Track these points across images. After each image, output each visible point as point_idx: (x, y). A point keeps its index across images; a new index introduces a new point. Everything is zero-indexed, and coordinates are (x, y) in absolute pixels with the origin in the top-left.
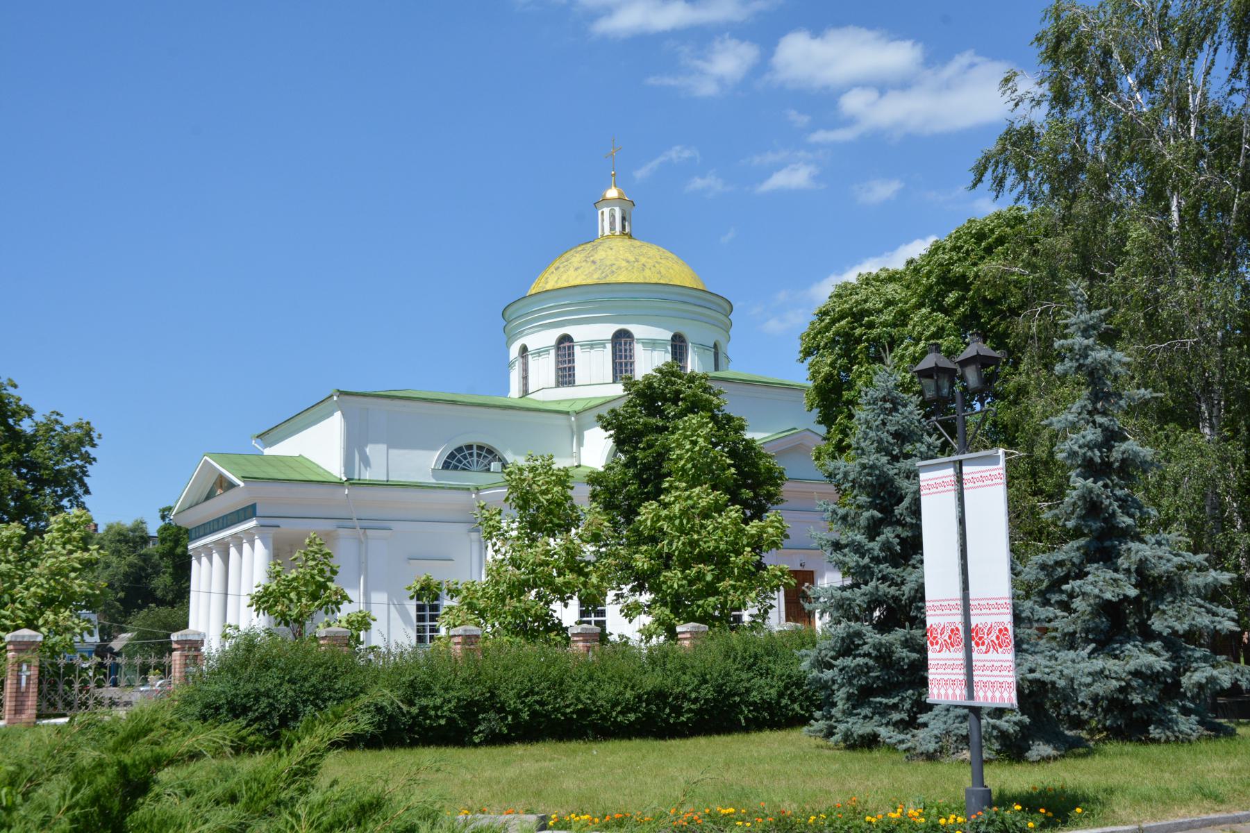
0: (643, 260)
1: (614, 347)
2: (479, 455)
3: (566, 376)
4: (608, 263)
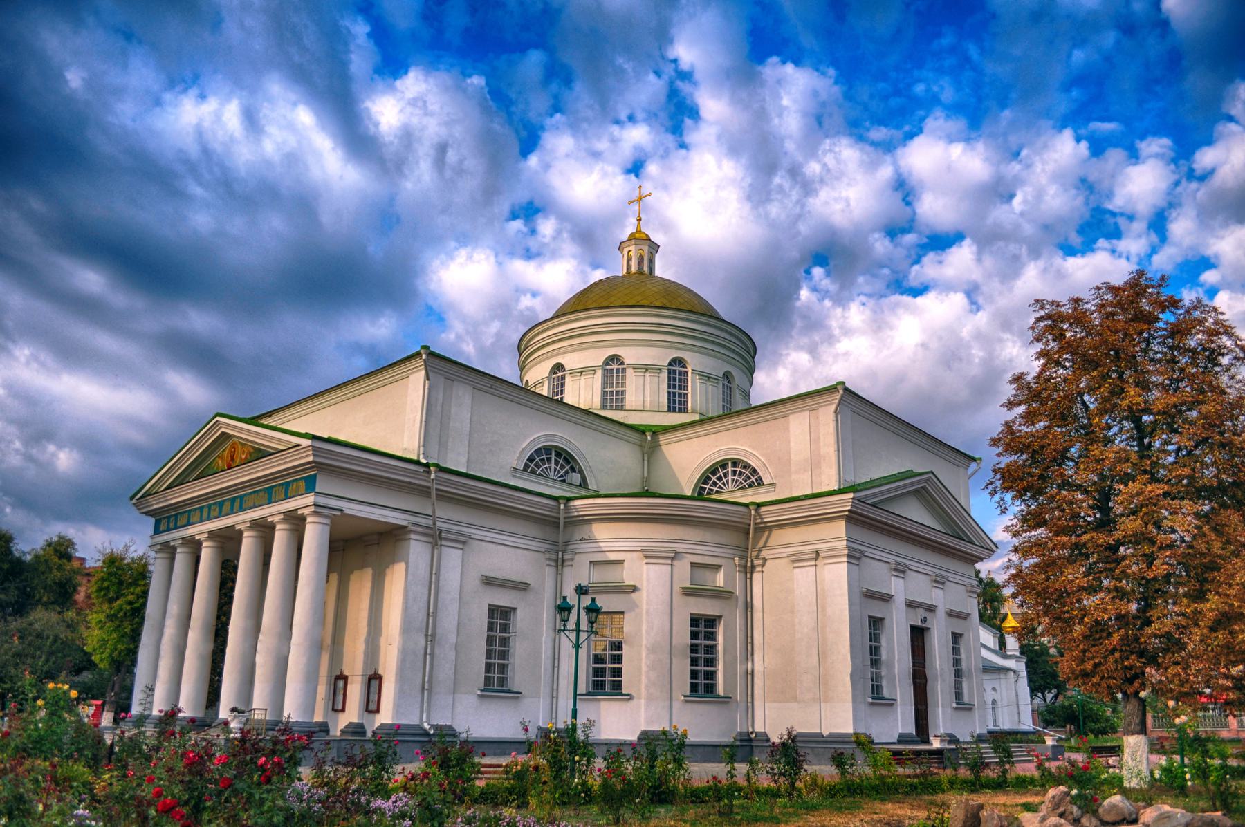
2: (557, 463)
3: (614, 397)
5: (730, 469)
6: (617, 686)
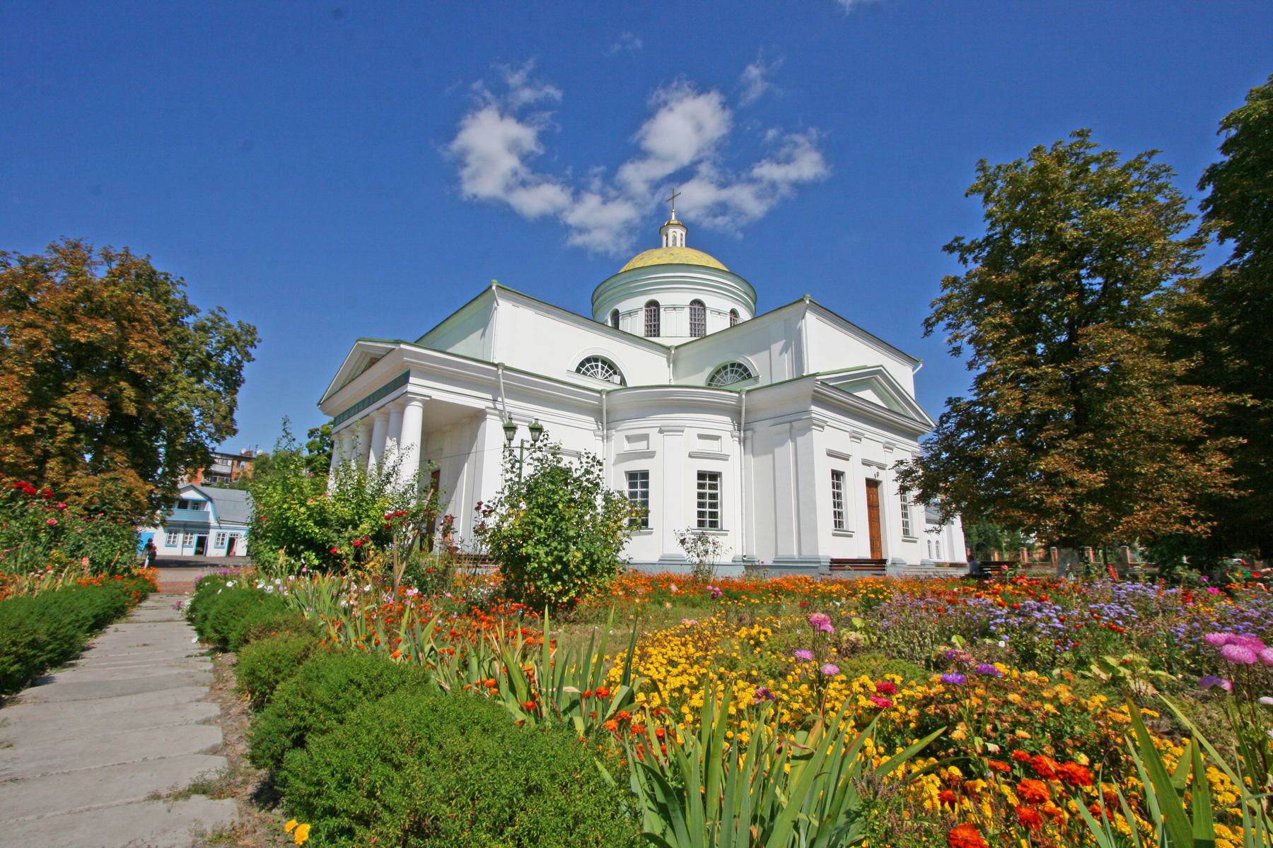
2: (603, 368)
5: (729, 369)
6: (645, 523)
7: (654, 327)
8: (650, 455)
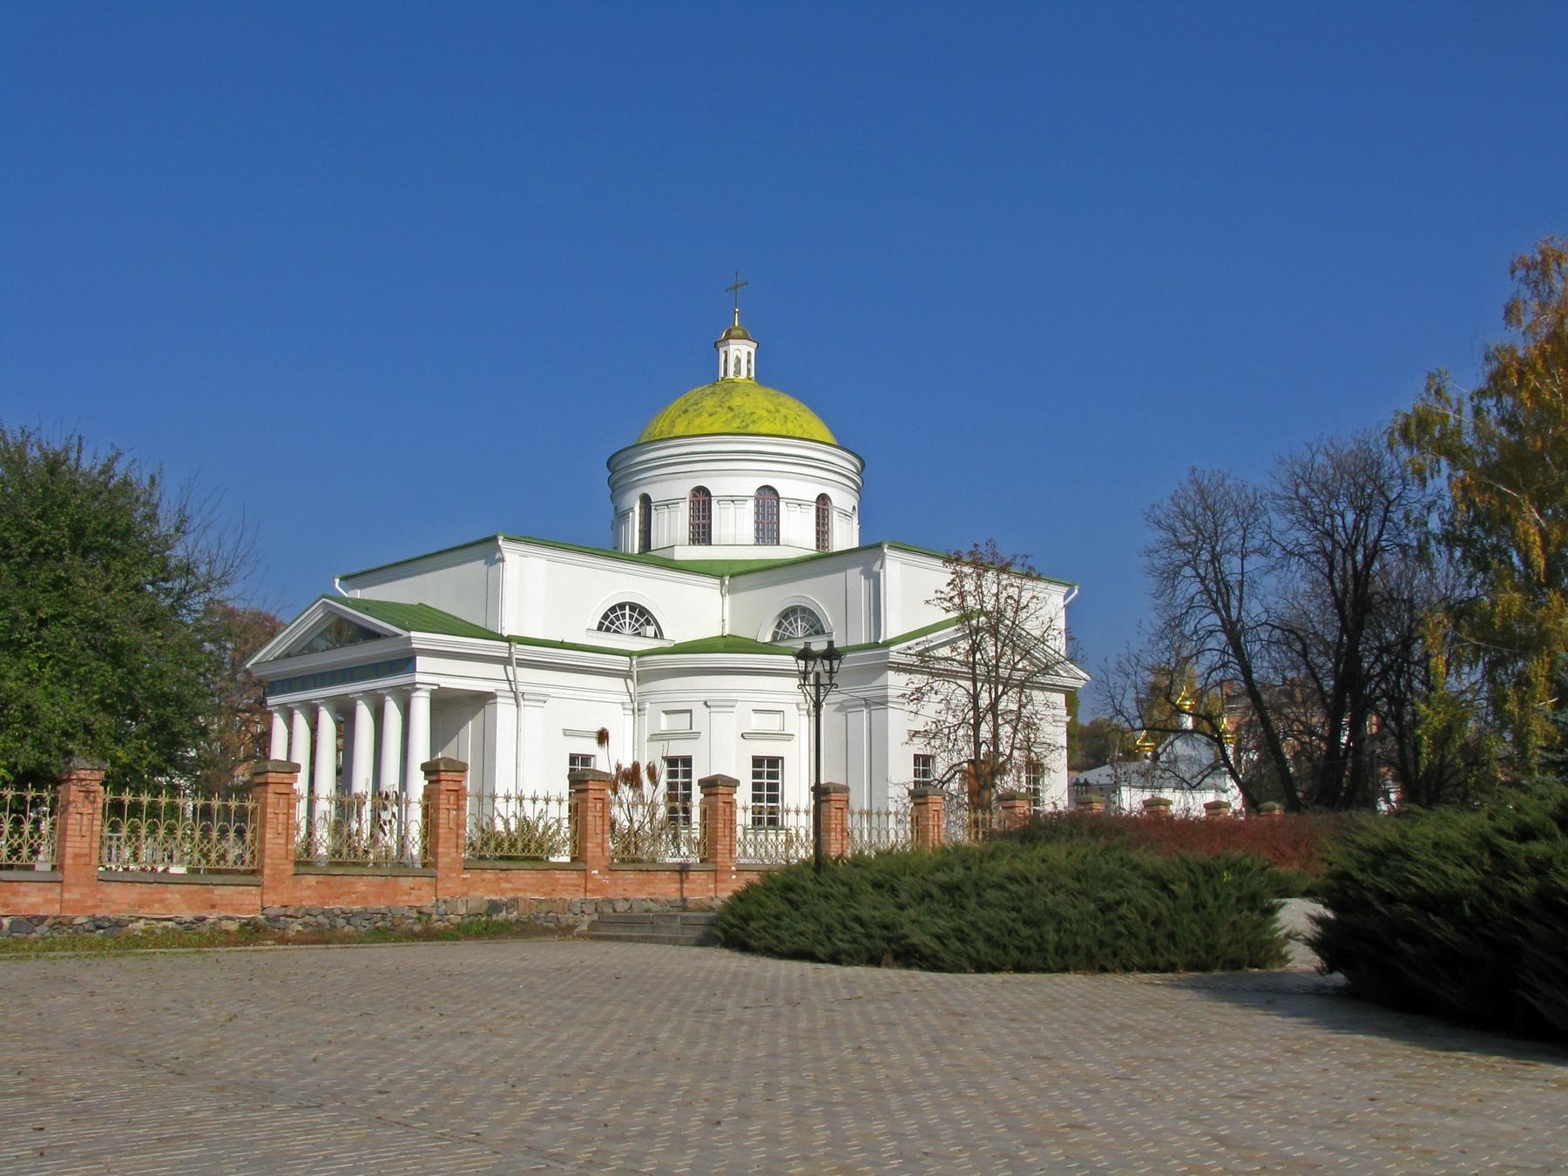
0: (784, 411)
1: (757, 506)
2: (631, 617)
4: (747, 411)
7: (701, 533)
8: (695, 736)
